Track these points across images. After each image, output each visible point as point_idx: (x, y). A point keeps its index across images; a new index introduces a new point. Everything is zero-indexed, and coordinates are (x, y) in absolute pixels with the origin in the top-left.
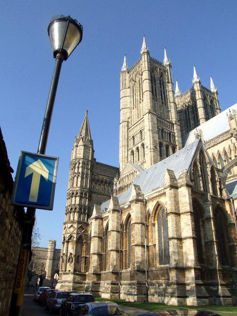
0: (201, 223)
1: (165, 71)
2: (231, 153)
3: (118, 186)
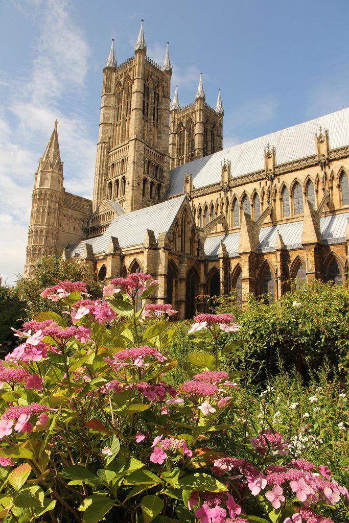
0: (174, 283)
2: (217, 208)
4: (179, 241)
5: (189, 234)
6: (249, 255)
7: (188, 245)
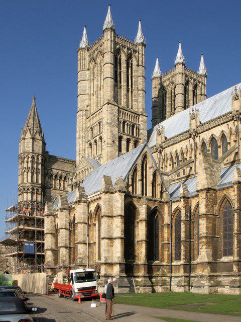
1: (135, 51)
3: (74, 181)
4: (139, 184)
5: (150, 178)
6: (205, 191)
7: (149, 188)
